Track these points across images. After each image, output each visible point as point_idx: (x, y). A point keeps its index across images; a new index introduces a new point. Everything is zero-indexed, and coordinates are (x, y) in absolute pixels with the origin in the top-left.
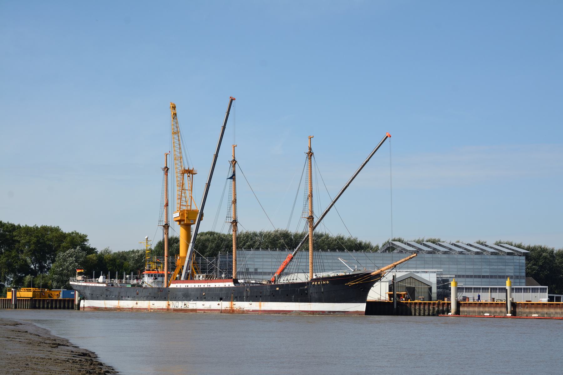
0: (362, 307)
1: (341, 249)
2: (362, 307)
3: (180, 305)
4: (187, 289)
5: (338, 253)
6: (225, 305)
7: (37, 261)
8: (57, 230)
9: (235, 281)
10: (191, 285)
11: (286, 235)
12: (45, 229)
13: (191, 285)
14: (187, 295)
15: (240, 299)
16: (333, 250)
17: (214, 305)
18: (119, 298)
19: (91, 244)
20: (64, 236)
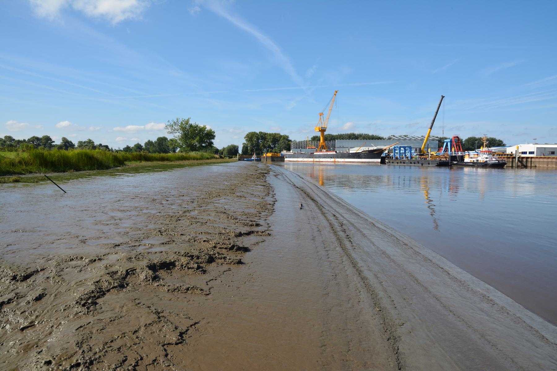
0: (379, 160)
1: (372, 139)
2: (379, 160)
3: (317, 160)
4: (320, 155)
5: (371, 140)
6: (332, 160)
7: (273, 144)
8: (279, 134)
9: (336, 152)
10: (321, 153)
11: (354, 135)
12: (275, 134)
13: (321, 153)
14: (320, 157)
15: (338, 158)
16: (369, 139)
17: (329, 160)
18: (298, 157)
19: (290, 138)
20: (281, 136)
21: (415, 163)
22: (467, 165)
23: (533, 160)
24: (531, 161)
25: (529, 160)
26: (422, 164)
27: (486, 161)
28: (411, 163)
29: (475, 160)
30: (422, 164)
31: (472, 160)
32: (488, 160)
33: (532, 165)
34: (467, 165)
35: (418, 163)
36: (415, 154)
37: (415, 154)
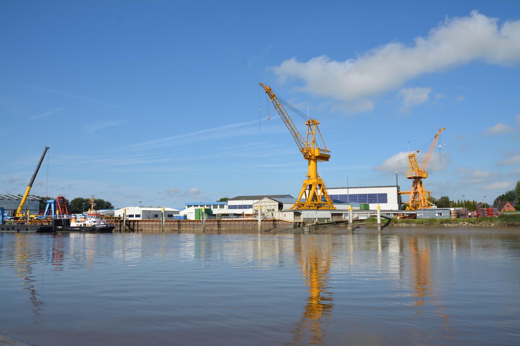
21: (8, 229)
22: (74, 230)
23: (139, 223)
24: (138, 225)
25: (136, 223)
26: (18, 231)
27: (94, 225)
28: (3, 229)
29: (82, 224)
30: (18, 231)
31: (79, 224)
32: (96, 224)
33: (139, 228)
34: (74, 230)
35: (13, 228)
36: (9, 218)
37: (9, 218)
